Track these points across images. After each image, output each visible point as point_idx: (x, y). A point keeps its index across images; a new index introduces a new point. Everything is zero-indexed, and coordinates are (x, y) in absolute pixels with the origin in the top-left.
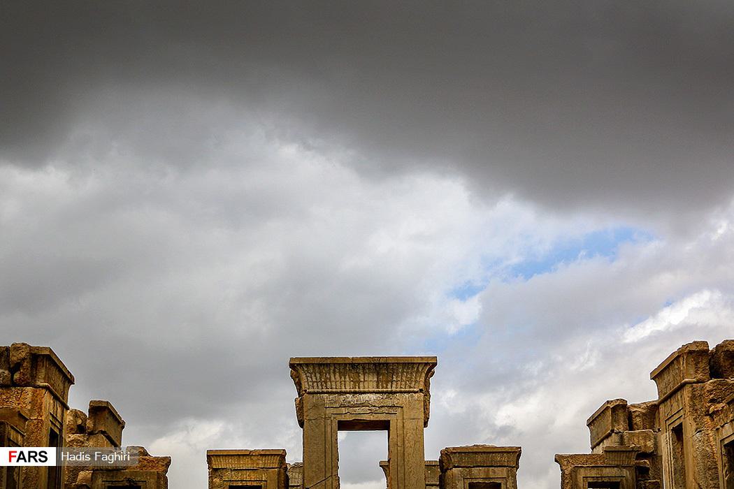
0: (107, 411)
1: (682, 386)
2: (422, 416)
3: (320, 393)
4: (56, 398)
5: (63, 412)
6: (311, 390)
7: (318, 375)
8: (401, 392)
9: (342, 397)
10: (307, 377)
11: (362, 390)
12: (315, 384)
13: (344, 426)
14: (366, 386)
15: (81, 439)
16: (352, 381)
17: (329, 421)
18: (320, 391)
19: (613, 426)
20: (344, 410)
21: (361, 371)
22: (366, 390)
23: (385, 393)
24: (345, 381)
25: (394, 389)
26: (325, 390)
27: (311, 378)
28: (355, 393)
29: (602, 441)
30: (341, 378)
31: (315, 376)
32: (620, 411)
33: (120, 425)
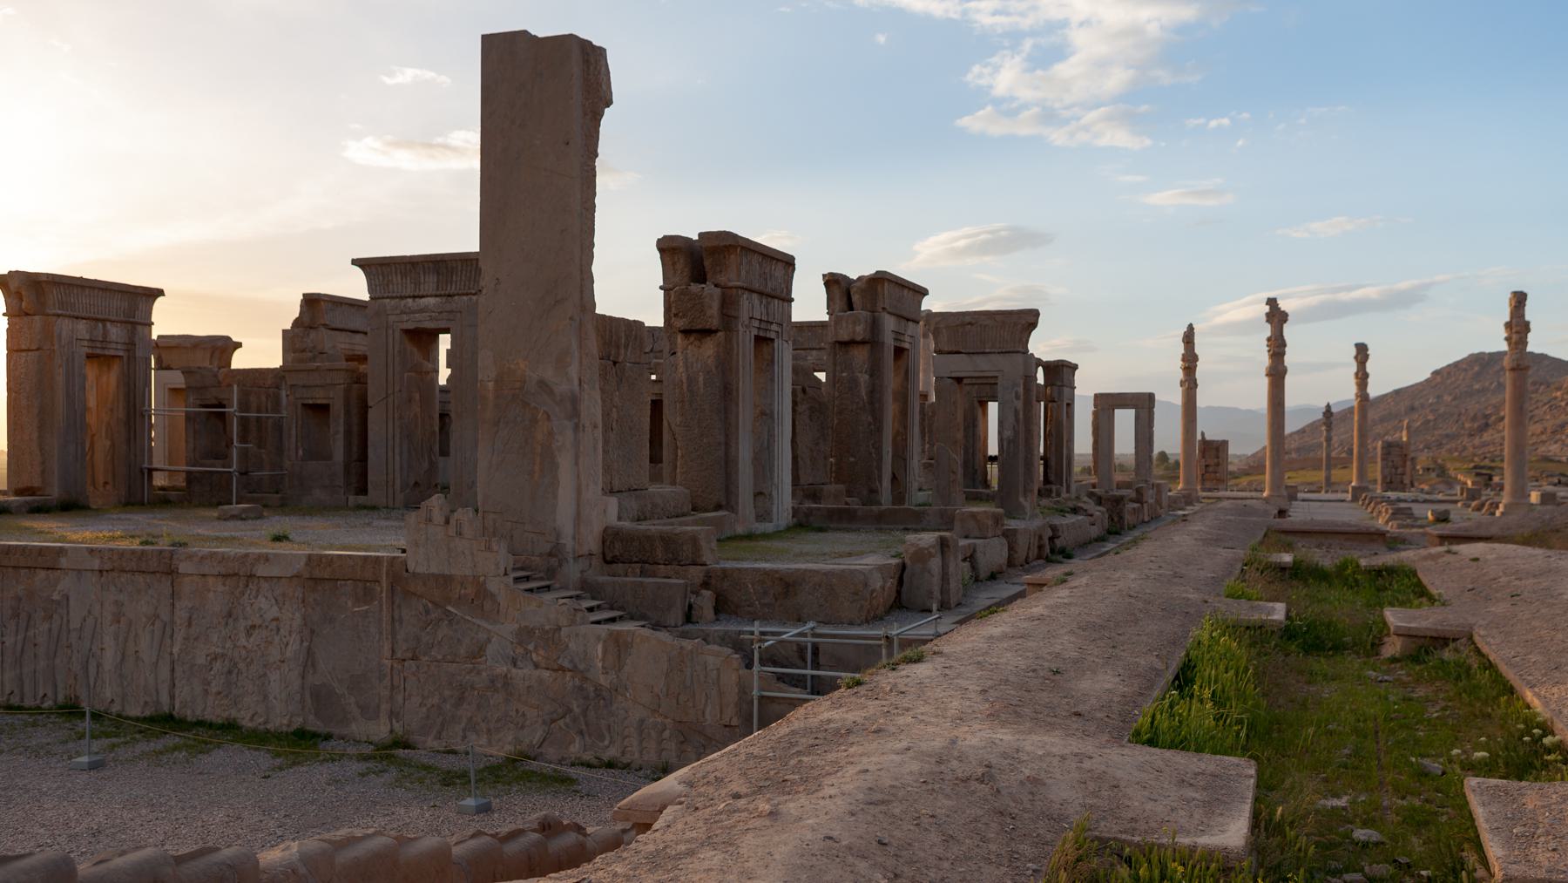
0: (322, 303)
3: (383, 298)
7: (381, 278)
8: (458, 295)
9: (403, 302)
11: (421, 293)
12: (378, 288)
14: (426, 288)
17: (391, 332)
20: (405, 317)
21: (421, 272)
22: (425, 294)
23: (445, 295)
24: (406, 283)
26: (386, 295)
30: (402, 279)
31: (379, 279)
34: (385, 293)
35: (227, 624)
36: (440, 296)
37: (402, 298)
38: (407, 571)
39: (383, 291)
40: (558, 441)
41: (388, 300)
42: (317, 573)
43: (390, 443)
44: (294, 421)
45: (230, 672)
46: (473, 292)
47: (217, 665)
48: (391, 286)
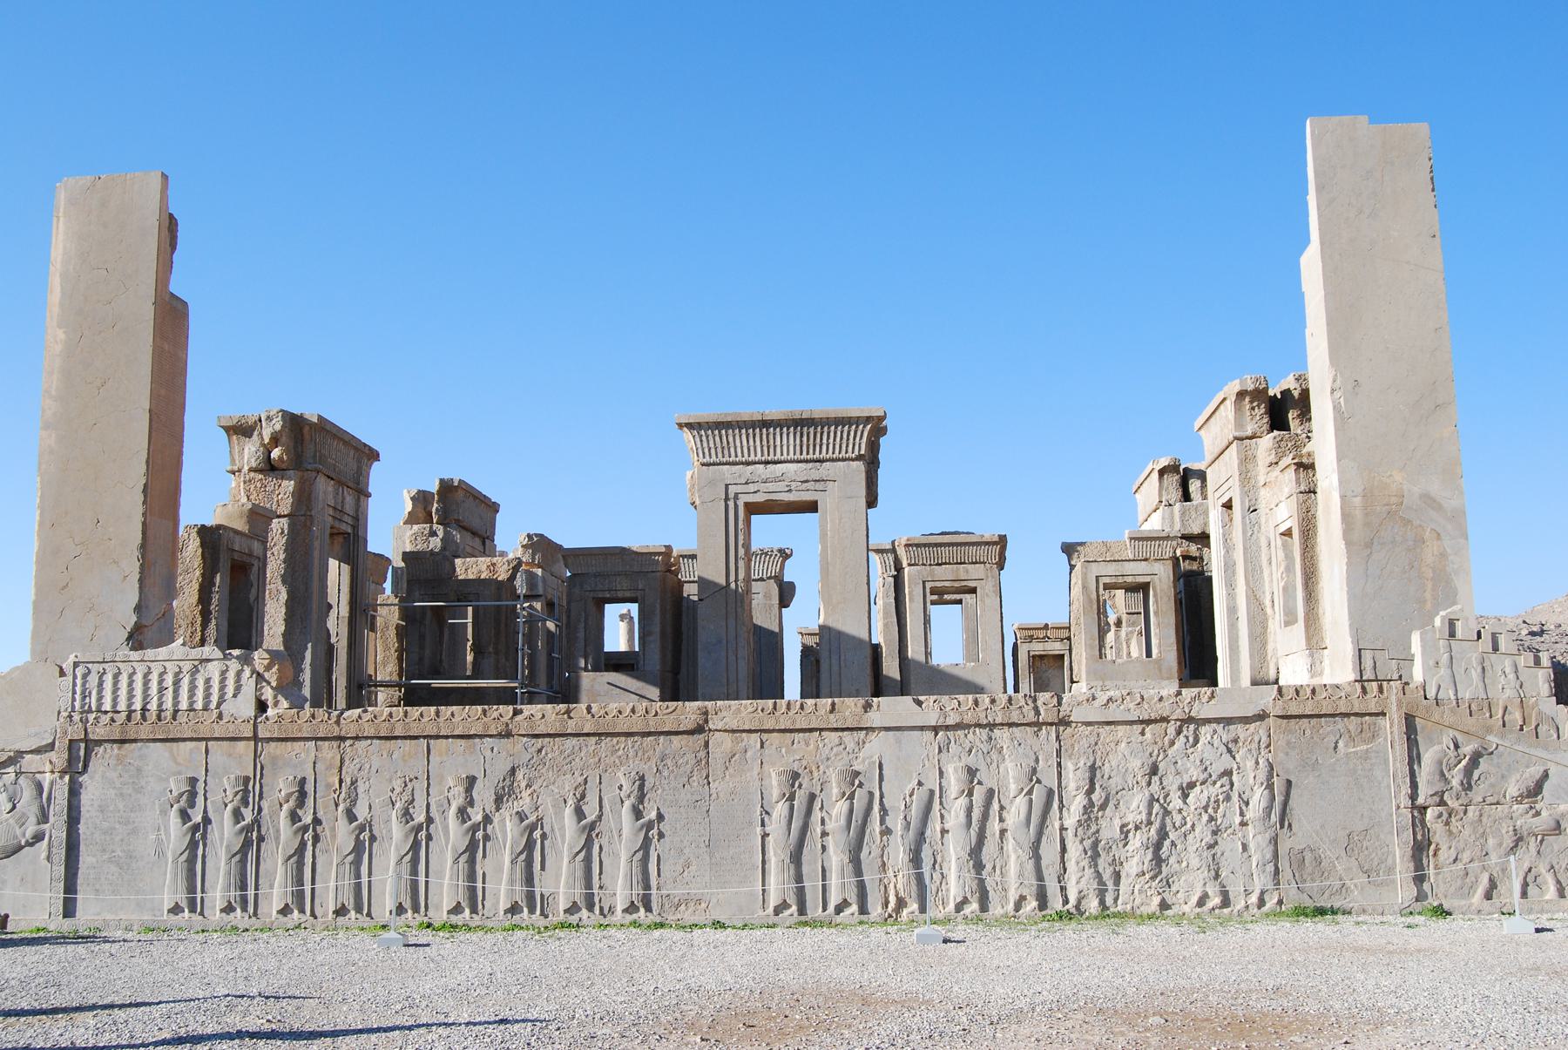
2: (863, 492)
20: (752, 488)
35: (1149, 784)
36: (807, 461)
37: (748, 463)
38: (1426, 698)
40: (1453, 563)
42: (1294, 709)
45: (1158, 846)
47: (1136, 841)
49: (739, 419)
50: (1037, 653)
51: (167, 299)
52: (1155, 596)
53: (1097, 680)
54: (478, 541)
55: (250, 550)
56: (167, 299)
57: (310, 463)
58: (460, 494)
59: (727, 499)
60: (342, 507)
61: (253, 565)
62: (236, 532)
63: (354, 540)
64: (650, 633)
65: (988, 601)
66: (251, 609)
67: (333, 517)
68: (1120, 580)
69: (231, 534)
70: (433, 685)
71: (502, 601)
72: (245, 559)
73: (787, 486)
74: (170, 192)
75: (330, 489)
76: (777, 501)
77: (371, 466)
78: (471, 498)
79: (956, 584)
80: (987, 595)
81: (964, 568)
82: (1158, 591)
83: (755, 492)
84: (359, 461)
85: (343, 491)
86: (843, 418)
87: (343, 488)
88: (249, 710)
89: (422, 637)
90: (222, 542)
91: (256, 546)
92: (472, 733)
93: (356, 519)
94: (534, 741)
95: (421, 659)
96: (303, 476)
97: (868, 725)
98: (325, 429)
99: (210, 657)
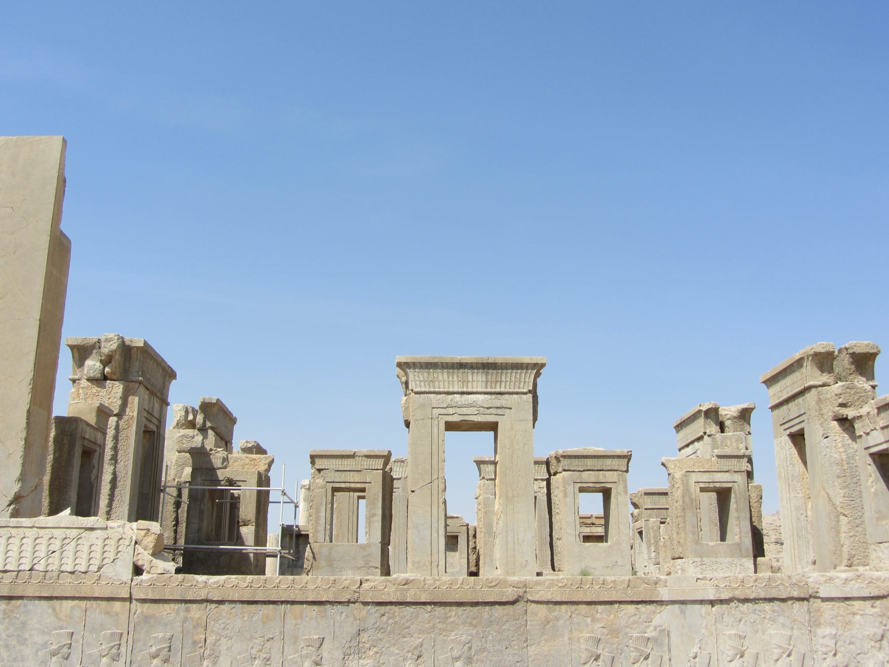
1: (808, 389)
4: (152, 393)
5: (161, 408)
6: (418, 389)
7: (426, 375)
9: (450, 397)
10: (414, 376)
11: (470, 390)
12: (422, 383)
13: (451, 426)
15: (191, 434)
16: (460, 381)
17: (436, 421)
18: (427, 390)
19: (705, 428)
20: (451, 411)
22: (474, 390)
24: (453, 381)
25: (503, 390)
26: (432, 390)
27: (419, 377)
28: (463, 393)
29: (692, 442)
30: (448, 377)
32: (712, 414)
33: (233, 421)
34: (430, 388)
39: (427, 386)
41: (435, 395)
43: (435, 525)
44: (324, 503)
46: (525, 391)
48: (437, 383)
49: (443, 361)
50: (586, 534)
51: (58, 235)
52: (736, 496)
53: (697, 557)
54: (223, 442)
55: (95, 438)
56: (58, 235)
57: (134, 376)
58: (215, 409)
59: (432, 418)
60: (152, 411)
61: (96, 451)
62: (88, 425)
63: (157, 435)
64: (374, 515)
65: (620, 498)
66: (92, 486)
67: (146, 418)
68: (712, 485)
69: (85, 426)
70: (244, 551)
71: (209, 490)
72: (92, 446)
73: (477, 410)
74: (67, 153)
75: (147, 397)
76: (469, 421)
77: (170, 383)
78: (222, 413)
79: (598, 485)
80: (620, 494)
81: (603, 474)
82: (738, 494)
83: (454, 414)
84: (164, 378)
85: (154, 399)
86: (517, 363)
87: (154, 397)
88: (126, 573)
89: (202, 513)
90: (78, 432)
91: (99, 435)
92: (324, 599)
93: (160, 421)
94: (377, 608)
95: (200, 530)
96: (129, 386)
97: (659, 599)
98: (147, 351)
99: (94, 526)
